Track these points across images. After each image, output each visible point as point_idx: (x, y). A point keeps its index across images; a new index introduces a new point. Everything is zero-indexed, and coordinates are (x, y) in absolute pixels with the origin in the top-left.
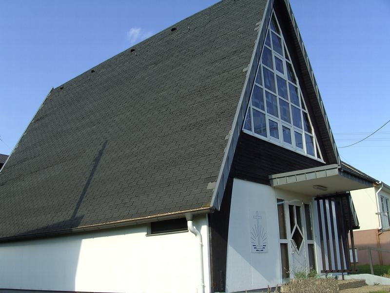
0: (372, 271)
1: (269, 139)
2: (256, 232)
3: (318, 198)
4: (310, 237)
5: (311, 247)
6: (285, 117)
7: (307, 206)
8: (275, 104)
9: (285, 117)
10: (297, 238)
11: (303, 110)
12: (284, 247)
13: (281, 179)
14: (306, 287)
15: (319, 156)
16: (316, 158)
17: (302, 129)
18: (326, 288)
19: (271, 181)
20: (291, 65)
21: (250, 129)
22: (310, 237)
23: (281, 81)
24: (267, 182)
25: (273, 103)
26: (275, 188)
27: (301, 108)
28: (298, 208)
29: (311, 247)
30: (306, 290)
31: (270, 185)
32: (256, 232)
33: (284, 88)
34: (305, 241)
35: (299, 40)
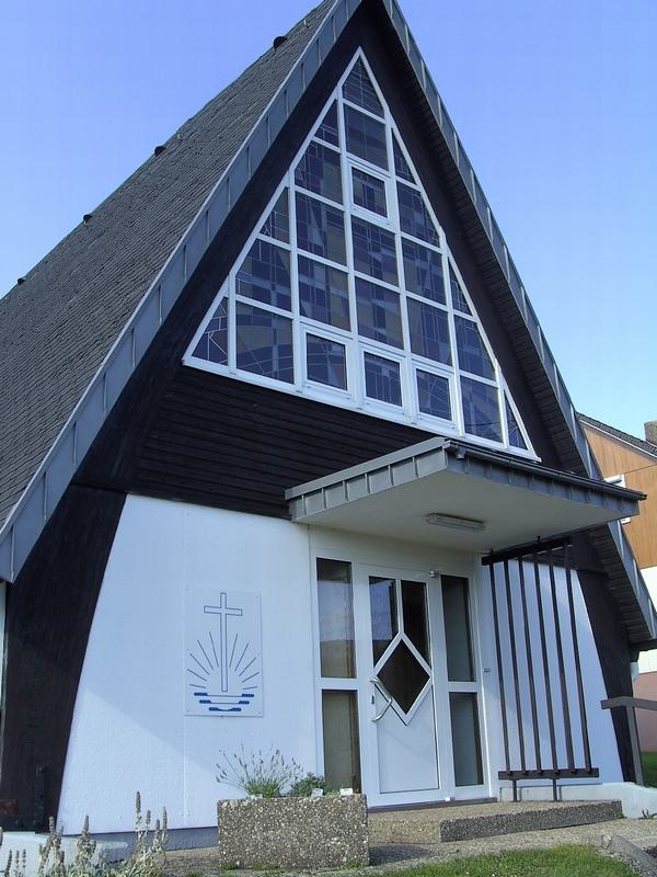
0: (639, 775)
1: (303, 386)
2: (209, 651)
3: (490, 560)
4: (462, 665)
5: (463, 705)
6: (380, 330)
7: (455, 589)
8: (342, 294)
9: (380, 330)
10: (403, 681)
11: (457, 308)
12: (340, 704)
13: (324, 497)
14: (266, 829)
15: (516, 439)
16: (504, 445)
17: (449, 363)
18: (328, 836)
19: (291, 505)
20: (419, 193)
21: (221, 358)
22: (462, 665)
23: (372, 242)
24: (279, 508)
25: (333, 290)
26: (308, 527)
27: (449, 307)
28: (414, 593)
29: (463, 705)
30: (267, 839)
31: (290, 520)
32: (209, 651)
33: (384, 251)
34: (438, 685)
35: (424, 87)
